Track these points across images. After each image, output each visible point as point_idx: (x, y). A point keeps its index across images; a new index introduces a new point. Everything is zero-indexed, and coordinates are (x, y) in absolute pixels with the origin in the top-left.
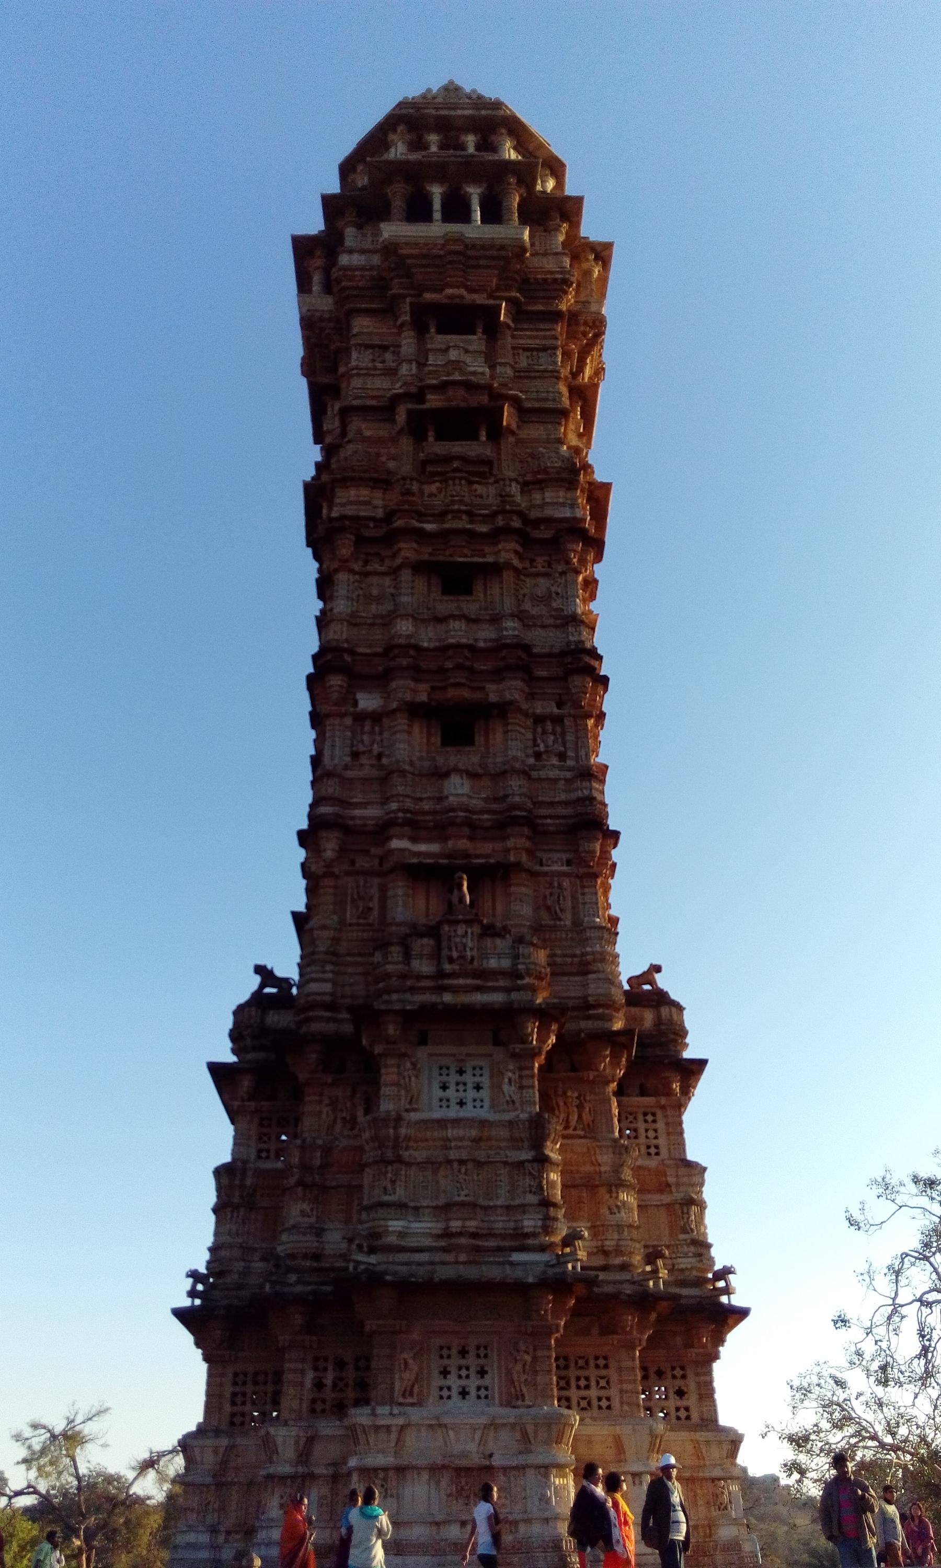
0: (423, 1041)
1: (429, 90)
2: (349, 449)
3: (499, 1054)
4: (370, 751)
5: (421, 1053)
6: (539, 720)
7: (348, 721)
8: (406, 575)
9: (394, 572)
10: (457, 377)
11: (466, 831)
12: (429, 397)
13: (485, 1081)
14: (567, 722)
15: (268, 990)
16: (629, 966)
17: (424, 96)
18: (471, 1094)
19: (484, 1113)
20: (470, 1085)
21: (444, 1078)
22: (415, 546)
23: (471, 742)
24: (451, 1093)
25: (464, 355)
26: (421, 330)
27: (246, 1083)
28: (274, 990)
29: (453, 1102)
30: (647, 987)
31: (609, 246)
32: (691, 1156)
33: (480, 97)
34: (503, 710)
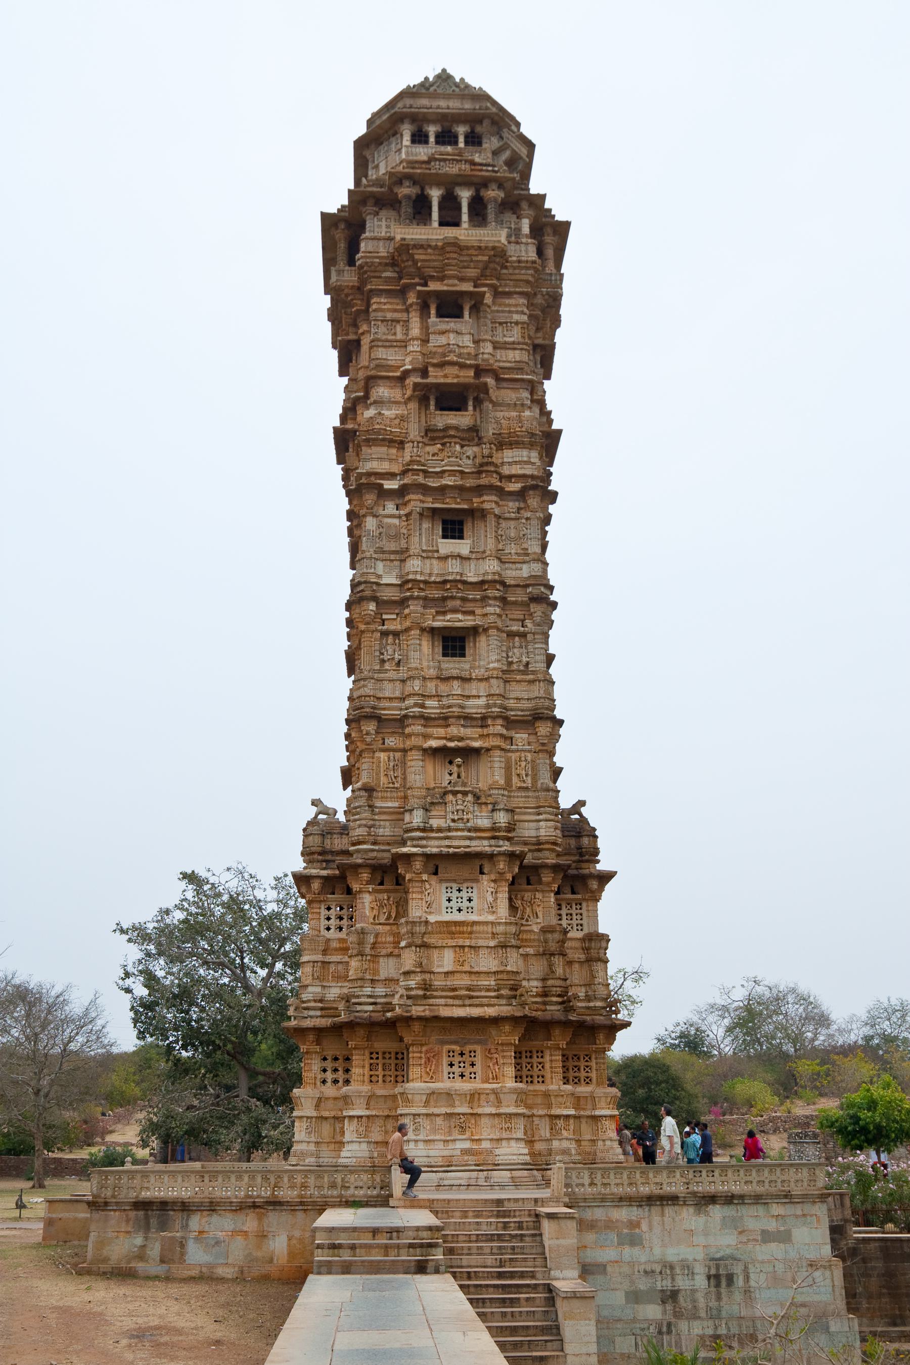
1: (426, 79)
2: (371, 412)
4: (393, 659)
6: (511, 635)
10: (452, 358)
15: (321, 816)
16: (565, 802)
17: (422, 85)
20: (465, 900)
21: (449, 895)
22: (421, 497)
25: (457, 337)
26: (424, 308)
27: (316, 885)
28: (325, 817)
29: (454, 910)
30: (577, 816)
31: (567, 225)
33: (467, 86)
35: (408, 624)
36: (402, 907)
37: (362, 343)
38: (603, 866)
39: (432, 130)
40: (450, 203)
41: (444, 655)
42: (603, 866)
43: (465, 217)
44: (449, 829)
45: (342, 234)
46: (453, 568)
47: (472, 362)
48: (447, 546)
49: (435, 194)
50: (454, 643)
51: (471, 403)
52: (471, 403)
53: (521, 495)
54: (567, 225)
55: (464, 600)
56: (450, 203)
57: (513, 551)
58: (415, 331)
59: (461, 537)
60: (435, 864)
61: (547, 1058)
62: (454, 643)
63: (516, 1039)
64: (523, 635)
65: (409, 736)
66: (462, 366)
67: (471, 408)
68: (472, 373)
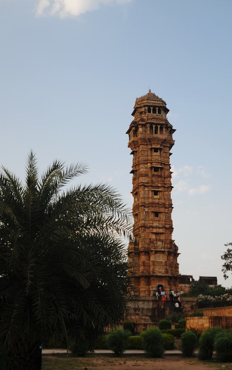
0: (156, 253)
3: (163, 255)
5: (156, 255)
6: (166, 213)
7: (144, 212)
8: (150, 192)
9: (149, 191)
10: (156, 161)
11: (158, 228)
12: (153, 163)
13: (162, 257)
14: (169, 213)
18: (160, 259)
19: (162, 261)
22: (151, 188)
23: (158, 217)
24: (159, 258)
32: (178, 263)
34: (162, 212)
35: (149, 211)
36: (149, 258)
37: (138, 152)
38: (178, 252)
39: (152, 108)
40: (156, 128)
41: (155, 216)
42: (178, 252)
43: (159, 132)
44: (158, 247)
45: (133, 129)
46: (157, 201)
47: (161, 162)
48: (155, 197)
49: (154, 126)
50: (157, 214)
51: (160, 170)
52: (160, 170)
53: (168, 187)
54: (175, 130)
55: (159, 207)
56: (156, 128)
57: (166, 198)
58: (149, 154)
59: (157, 195)
60: (156, 252)
61: (171, 283)
62: (157, 214)
63: (168, 279)
64: (168, 213)
65: (150, 230)
66: (159, 163)
67: (160, 171)
68: (160, 164)
